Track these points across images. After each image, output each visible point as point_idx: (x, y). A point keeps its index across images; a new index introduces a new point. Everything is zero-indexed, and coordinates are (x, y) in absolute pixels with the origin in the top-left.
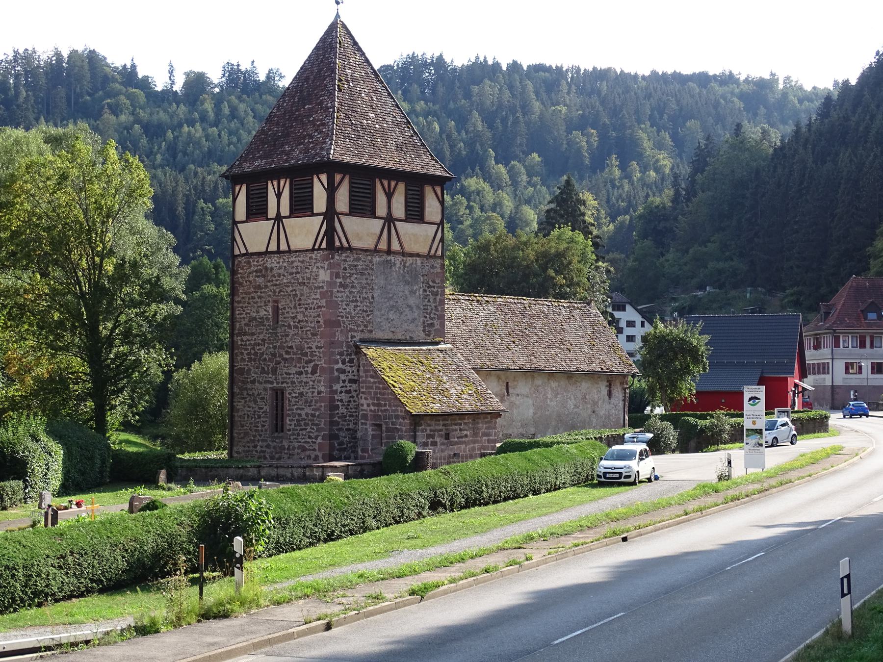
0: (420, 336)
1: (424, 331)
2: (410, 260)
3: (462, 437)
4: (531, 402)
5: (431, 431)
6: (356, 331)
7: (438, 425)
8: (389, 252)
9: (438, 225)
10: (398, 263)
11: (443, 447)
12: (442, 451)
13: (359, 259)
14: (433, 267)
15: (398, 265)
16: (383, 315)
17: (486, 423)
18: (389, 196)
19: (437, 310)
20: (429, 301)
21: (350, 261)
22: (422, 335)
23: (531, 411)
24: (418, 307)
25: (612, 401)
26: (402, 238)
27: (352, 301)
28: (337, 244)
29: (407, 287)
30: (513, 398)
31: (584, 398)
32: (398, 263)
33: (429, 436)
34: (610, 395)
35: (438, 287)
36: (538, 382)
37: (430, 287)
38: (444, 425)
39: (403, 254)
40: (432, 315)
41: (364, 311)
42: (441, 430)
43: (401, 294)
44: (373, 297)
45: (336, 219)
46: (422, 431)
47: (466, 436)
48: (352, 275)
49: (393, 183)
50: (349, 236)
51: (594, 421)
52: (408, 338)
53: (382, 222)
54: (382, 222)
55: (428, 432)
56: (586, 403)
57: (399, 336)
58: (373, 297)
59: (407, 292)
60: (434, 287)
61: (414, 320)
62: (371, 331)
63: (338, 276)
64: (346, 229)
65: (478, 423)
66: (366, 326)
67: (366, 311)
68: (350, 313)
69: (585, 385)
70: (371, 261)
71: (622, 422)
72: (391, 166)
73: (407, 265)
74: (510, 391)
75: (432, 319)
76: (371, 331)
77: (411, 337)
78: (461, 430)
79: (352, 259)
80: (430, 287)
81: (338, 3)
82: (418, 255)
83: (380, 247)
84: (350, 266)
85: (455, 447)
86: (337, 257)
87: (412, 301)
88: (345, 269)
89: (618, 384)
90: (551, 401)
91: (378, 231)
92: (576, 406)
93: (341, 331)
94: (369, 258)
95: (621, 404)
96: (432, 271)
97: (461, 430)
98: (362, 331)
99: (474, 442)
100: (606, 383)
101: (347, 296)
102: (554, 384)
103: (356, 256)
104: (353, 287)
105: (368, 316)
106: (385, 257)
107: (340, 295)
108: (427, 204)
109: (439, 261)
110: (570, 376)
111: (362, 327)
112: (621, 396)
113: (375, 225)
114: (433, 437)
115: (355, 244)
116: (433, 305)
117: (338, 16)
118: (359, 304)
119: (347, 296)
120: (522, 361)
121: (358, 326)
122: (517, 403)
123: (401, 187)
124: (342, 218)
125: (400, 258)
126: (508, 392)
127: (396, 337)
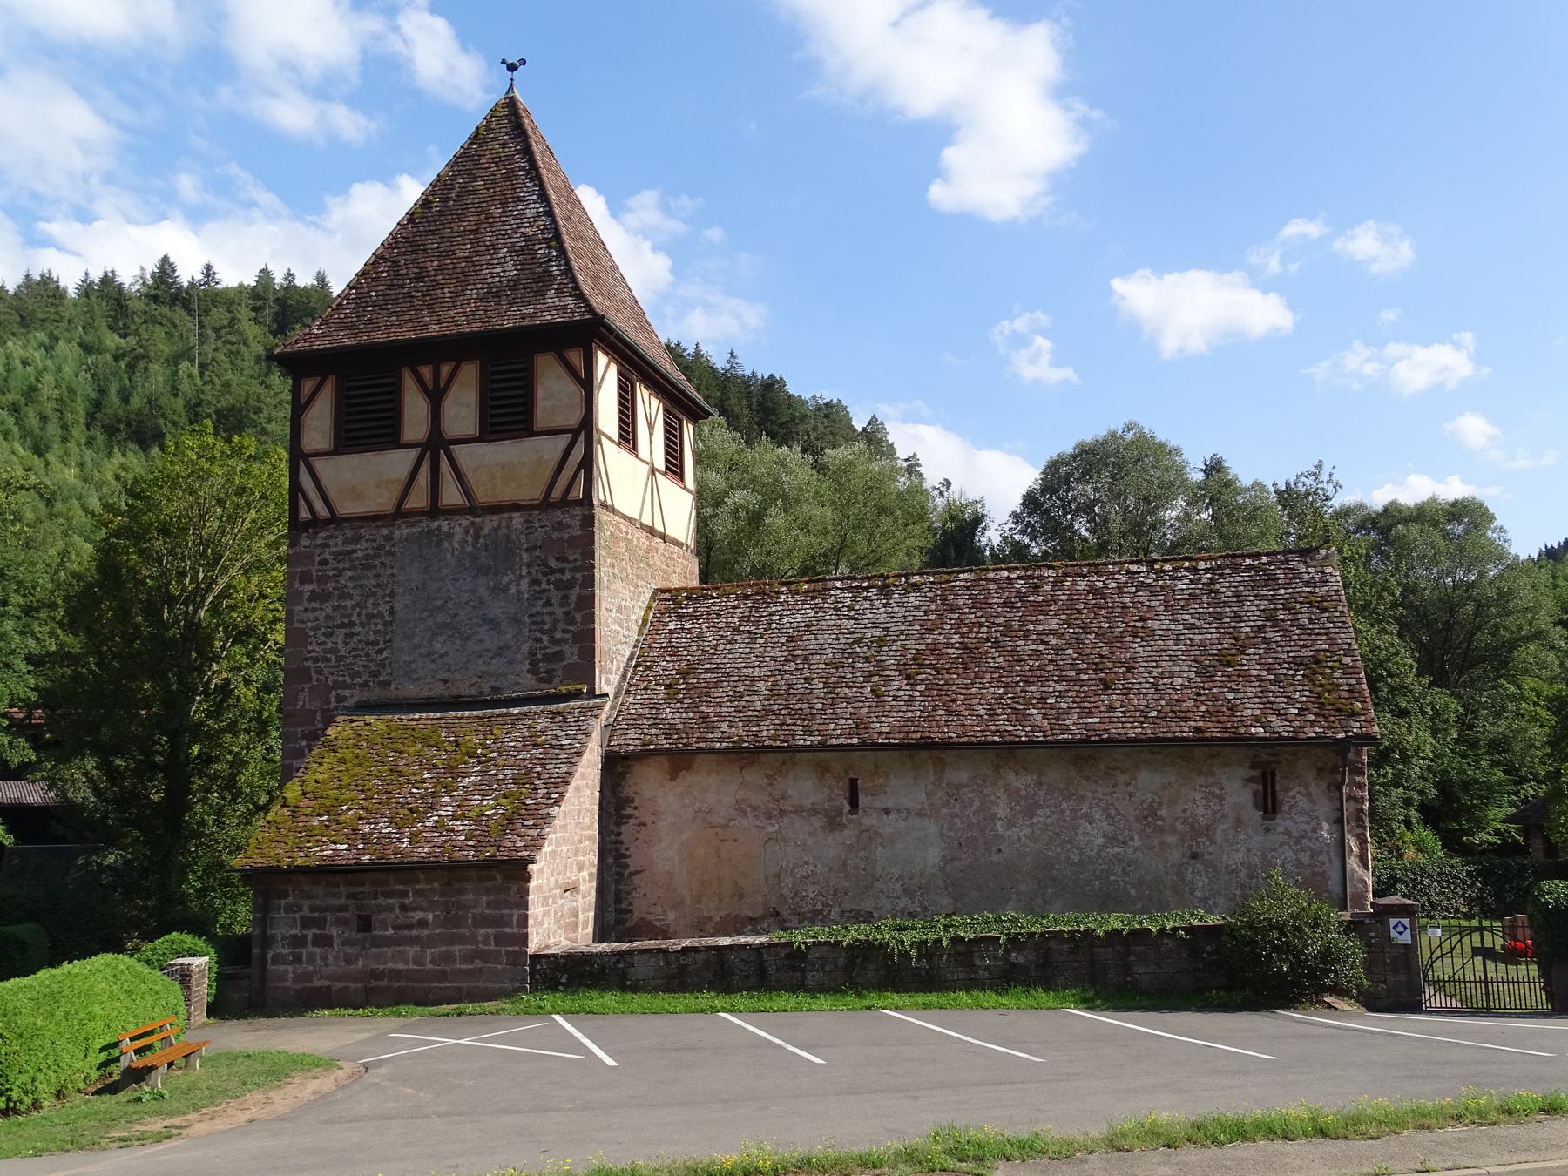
0: (529, 684)
1: (534, 671)
2: (491, 522)
3: (409, 927)
4: (932, 828)
5: (313, 909)
6: (349, 687)
7: (335, 895)
8: (435, 510)
9: (575, 433)
10: (458, 532)
11: (349, 950)
12: (348, 961)
13: (357, 539)
14: (559, 526)
15: (458, 537)
16: (417, 647)
17: (488, 891)
18: (436, 396)
19: (571, 621)
20: (548, 603)
21: (338, 544)
22: (530, 680)
23: (934, 855)
24: (515, 620)
25: (1281, 823)
26: (470, 477)
27: (339, 626)
28: (304, 514)
29: (482, 580)
30: (870, 820)
31: (1149, 815)
32: (458, 532)
33: (307, 923)
34: (1269, 805)
35: (574, 570)
36: (959, 774)
37: (552, 571)
38: (350, 896)
39: (472, 509)
40: (558, 635)
41: (368, 643)
42: (344, 908)
43: (466, 597)
44: (392, 612)
45: (303, 468)
46: (289, 909)
47: (422, 924)
48: (340, 573)
49: (446, 369)
50: (332, 494)
51: (1201, 882)
52: (486, 689)
53: (413, 453)
54: (413, 453)
55: (306, 912)
56: (1161, 830)
57: (463, 689)
58: (392, 612)
59: (483, 591)
60: (562, 571)
61: (501, 651)
62: (386, 684)
63: (305, 578)
64: (324, 482)
65: (461, 892)
66: (375, 674)
67: (375, 643)
68: (334, 651)
69: (1149, 781)
70: (388, 538)
71: (1334, 883)
72: (434, 330)
73: (486, 531)
74: (863, 800)
75: (554, 642)
76: (386, 684)
77: (495, 690)
78: (404, 908)
79: (339, 541)
80: (552, 571)
81: (512, 68)
82: (515, 507)
83: (411, 503)
84: (336, 555)
85: (390, 951)
86: (304, 542)
87: (496, 609)
88: (324, 562)
89: (1310, 776)
90: (1010, 823)
91: (403, 473)
92: (1112, 839)
93: (312, 689)
94: (385, 531)
95: (1326, 832)
96: (556, 535)
97: (404, 908)
98: (365, 685)
99: (451, 940)
100: (1244, 771)
101: (328, 617)
102: (1020, 781)
103: (349, 533)
104: (343, 596)
105: (380, 652)
106: (424, 525)
107: (311, 616)
108: (540, 393)
109: (578, 511)
110: (1088, 753)
111: (365, 677)
112: (1324, 808)
113: (397, 463)
114: (320, 924)
115: (346, 508)
116: (559, 612)
117: (511, 87)
118: (358, 629)
119: (328, 617)
120: (882, 725)
121: (358, 674)
122: (886, 830)
123: (470, 373)
124: (318, 464)
125: (465, 521)
126: (854, 804)
127: (455, 692)
